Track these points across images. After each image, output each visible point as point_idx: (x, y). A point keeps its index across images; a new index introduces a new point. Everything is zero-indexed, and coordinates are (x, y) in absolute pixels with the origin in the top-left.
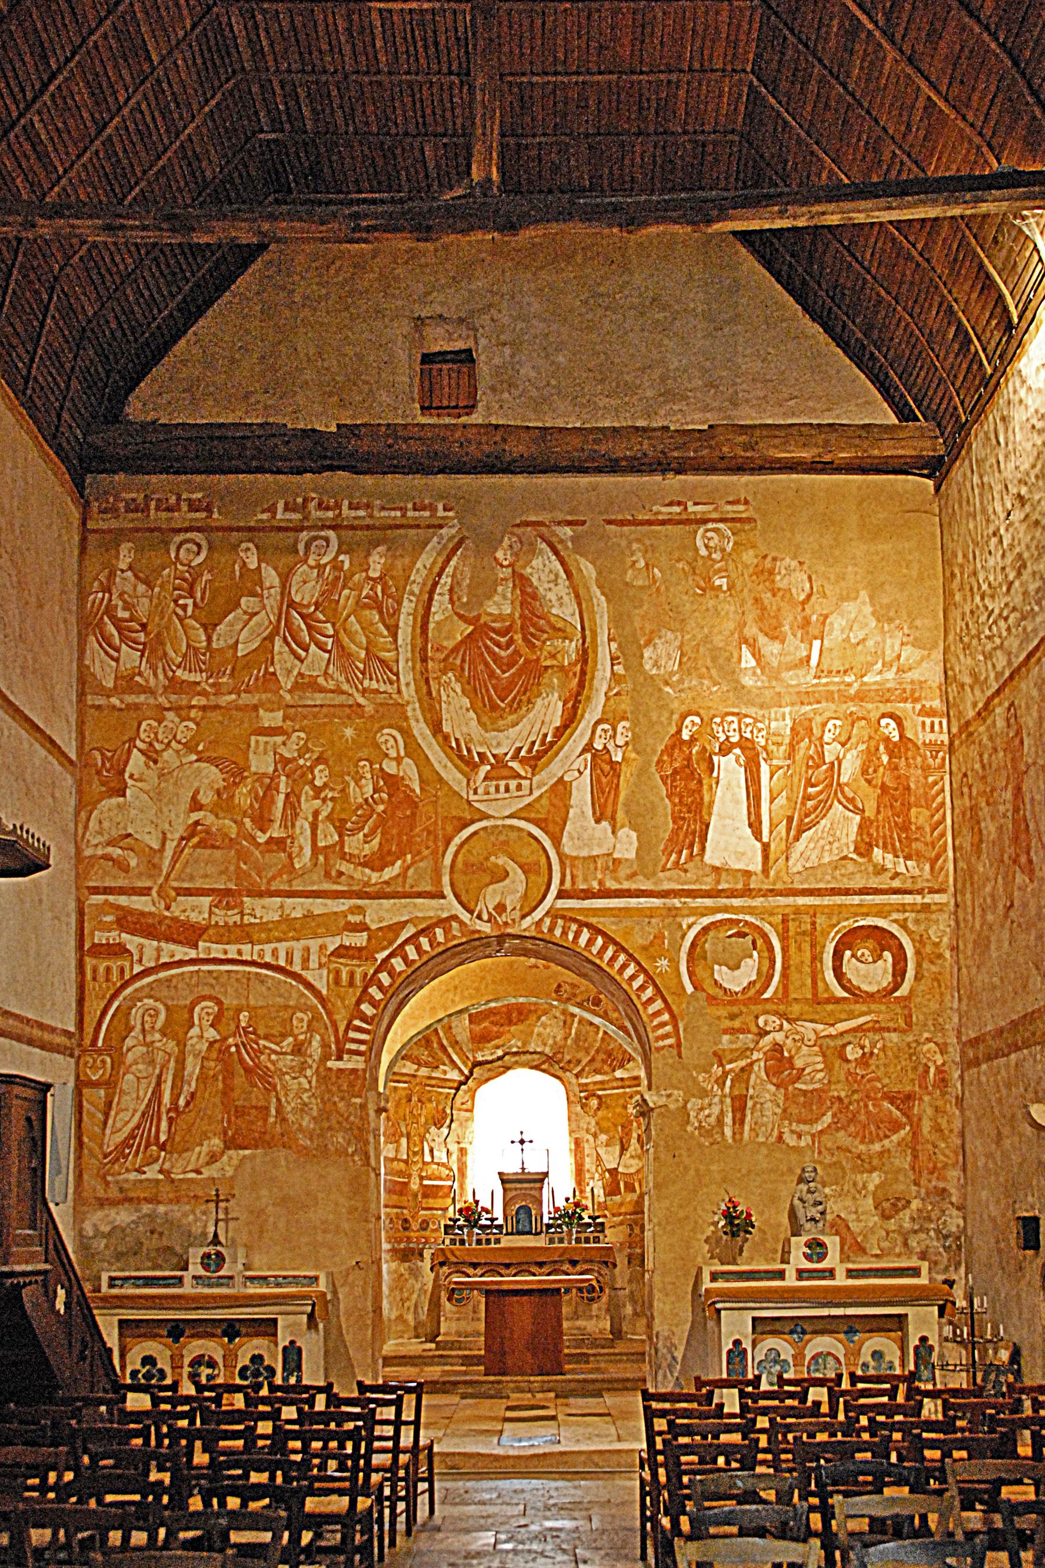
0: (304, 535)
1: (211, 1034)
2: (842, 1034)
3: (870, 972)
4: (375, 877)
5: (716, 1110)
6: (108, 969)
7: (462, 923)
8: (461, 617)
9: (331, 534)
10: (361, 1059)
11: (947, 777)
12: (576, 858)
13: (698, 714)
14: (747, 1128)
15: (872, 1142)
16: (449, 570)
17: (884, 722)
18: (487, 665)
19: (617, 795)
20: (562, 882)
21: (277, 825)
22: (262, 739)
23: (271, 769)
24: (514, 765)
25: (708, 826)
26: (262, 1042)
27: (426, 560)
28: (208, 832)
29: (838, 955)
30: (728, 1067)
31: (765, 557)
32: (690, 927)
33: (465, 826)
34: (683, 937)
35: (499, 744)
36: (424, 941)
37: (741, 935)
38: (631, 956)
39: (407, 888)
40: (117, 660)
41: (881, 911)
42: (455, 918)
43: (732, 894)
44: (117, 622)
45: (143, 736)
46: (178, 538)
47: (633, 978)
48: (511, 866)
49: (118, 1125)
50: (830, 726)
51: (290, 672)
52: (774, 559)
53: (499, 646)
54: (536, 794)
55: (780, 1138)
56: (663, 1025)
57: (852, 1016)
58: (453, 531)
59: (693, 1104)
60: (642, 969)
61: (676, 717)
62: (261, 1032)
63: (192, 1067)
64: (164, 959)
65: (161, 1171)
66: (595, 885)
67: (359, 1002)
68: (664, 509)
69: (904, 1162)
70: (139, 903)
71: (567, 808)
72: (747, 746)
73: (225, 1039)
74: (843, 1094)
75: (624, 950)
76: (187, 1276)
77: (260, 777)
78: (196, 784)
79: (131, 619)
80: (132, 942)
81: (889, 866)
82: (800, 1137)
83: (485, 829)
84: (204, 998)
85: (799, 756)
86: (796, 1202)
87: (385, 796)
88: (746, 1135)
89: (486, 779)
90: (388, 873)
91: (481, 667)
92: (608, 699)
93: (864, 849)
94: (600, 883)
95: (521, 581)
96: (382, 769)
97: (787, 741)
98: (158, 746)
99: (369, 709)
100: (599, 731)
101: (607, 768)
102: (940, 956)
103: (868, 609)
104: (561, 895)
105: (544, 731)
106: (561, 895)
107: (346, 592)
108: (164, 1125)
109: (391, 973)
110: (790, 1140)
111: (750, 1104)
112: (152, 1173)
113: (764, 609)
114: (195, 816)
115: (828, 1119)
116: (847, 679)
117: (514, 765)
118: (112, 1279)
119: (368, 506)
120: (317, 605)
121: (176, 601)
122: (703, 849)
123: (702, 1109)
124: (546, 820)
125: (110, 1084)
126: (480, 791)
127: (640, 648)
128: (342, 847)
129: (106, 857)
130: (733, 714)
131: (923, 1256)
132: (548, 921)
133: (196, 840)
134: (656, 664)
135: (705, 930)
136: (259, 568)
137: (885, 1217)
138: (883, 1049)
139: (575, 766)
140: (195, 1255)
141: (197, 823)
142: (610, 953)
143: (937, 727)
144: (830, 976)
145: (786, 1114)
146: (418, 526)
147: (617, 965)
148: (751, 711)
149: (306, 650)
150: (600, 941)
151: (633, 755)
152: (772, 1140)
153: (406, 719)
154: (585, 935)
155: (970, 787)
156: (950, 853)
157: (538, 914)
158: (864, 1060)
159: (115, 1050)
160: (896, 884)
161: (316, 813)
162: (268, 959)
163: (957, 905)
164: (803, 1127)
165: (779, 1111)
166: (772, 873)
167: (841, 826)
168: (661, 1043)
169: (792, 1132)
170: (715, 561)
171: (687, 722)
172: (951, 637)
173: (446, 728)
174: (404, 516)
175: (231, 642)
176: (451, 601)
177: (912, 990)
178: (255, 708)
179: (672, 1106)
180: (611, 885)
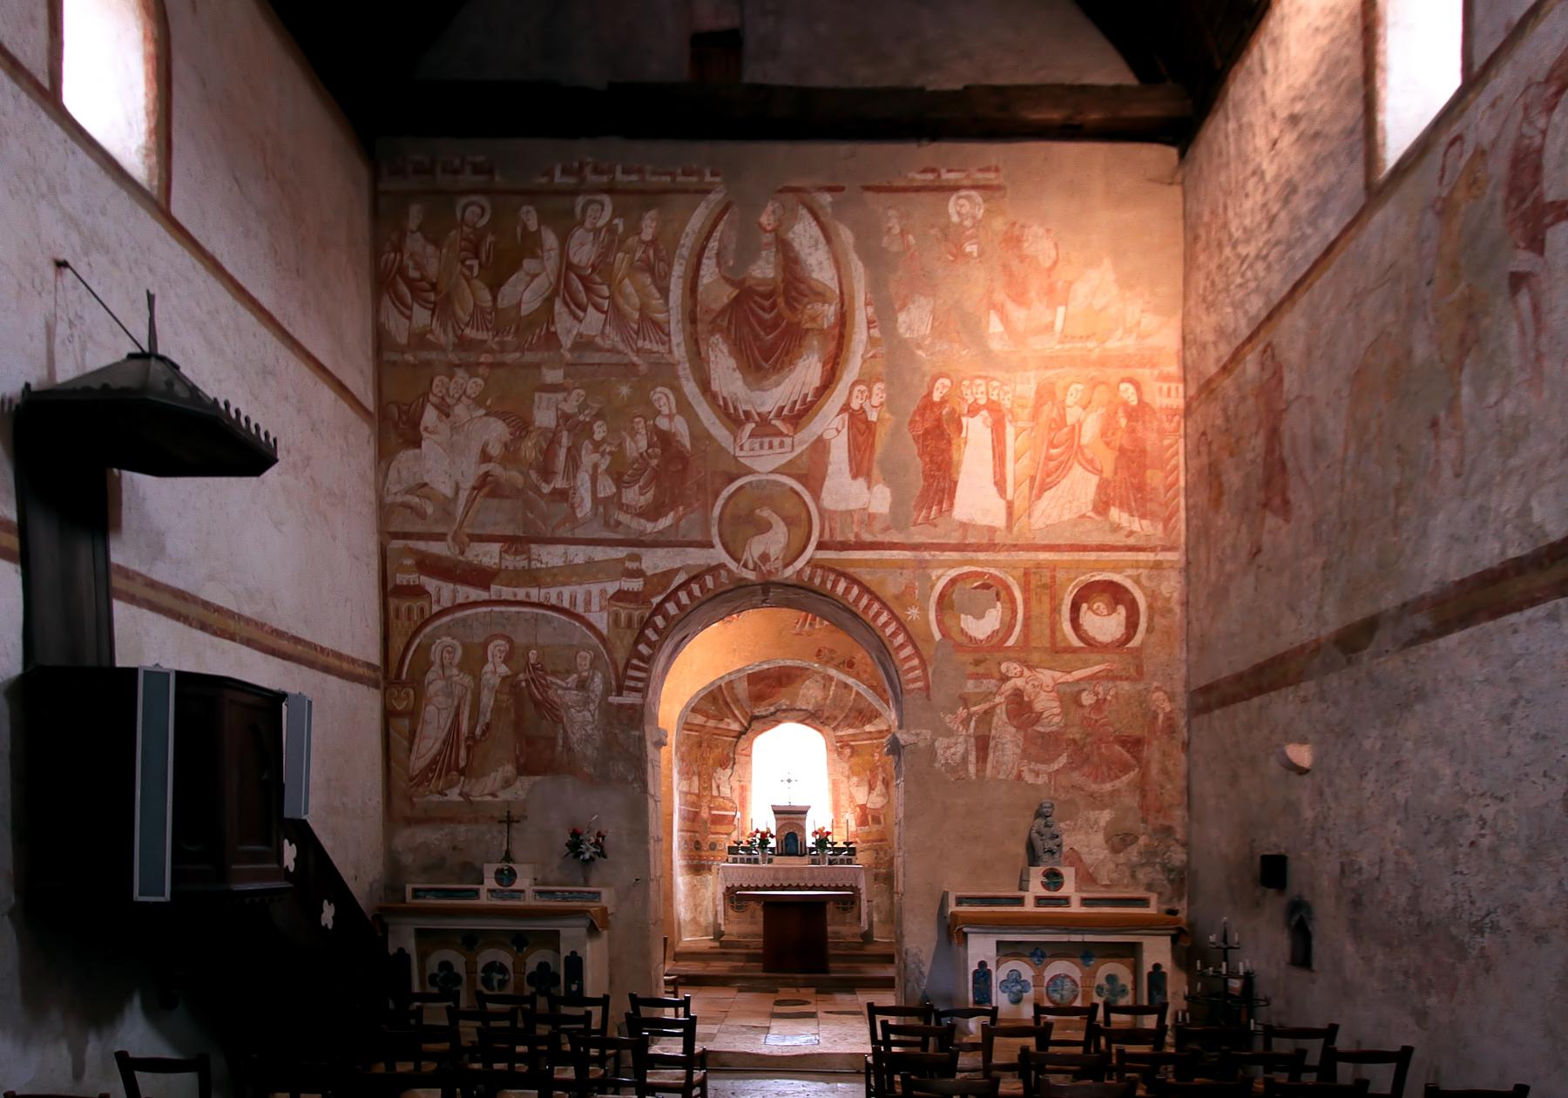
0: (581, 200)
1: (503, 669)
2: (1078, 681)
3: (1104, 624)
4: (649, 527)
5: (960, 749)
6: (410, 610)
7: (729, 571)
8: (727, 280)
9: (606, 199)
10: (638, 695)
11: (1182, 441)
12: (835, 512)
13: (948, 376)
14: (989, 766)
15: (1103, 781)
16: (717, 234)
17: (1123, 386)
18: (752, 328)
19: (872, 453)
20: (821, 535)
21: (559, 478)
22: (545, 396)
23: (553, 424)
24: (777, 423)
25: (956, 483)
26: (549, 678)
27: (697, 220)
28: (497, 483)
29: (1075, 608)
30: (973, 709)
31: (1014, 224)
32: (938, 578)
33: (732, 480)
34: (932, 587)
35: (763, 404)
36: (695, 588)
37: (986, 586)
38: (884, 605)
39: (680, 538)
40: (409, 318)
41: (1117, 567)
42: (723, 566)
43: (978, 548)
44: (410, 282)
45: (435, 390)
46: (463, 201)
47: (886, 625)
48: (776, 520)
49: (423, 751)
50: (1072, 388)
51: (569, 331)
52: (1023, 227)
53: (763, 309)
54: (798, 450)
55: (1019, 777)
56: (913, 669)
57: (1086, 665)
58: (720, 196)
59: (941, 743)
60: (894, 616)
61: (927, 379)
62: (549, 669)
63: (487, 700)
64: (460, 600)
65: (461, 794)
66: (852, 538)
67: (636, 643)
68: (919, 177)
69: (1131, 801)
70: (436, 548)
71: (826, 465)
72: (993, 408)
73: (517, 674)
74: (1078, 737)
75: (877, 598)
76: (483, 890)
77: (544, 431)
78: (485, 437)
79: (423, 279)
80: (431, 584)
81: (1125, 524)
82: (1038, 775)
83: (750, 483)
84: (496, 637)
85: (1043, 418)
86: (1035, 835)
87: (658, 450)
88: (988, 772)
89: (751, 436)
90: (665, 522)
91: (746, 330)
92: (864, 361)
93: (1102, 507)
94: (857, 535)
95: (785, 249)
96: (655, 425)
97: (1031, 403)
98: (448, 400)
99: (643, 368)
100: (856, 393)
101: (862, 427)
102: (1170, 610)
103: (1110, 276)
104: (821, 546)
105: (805, 391)
106: (821, 546)
107: (620, 255)
108: (463, 753)
109: (666, 617)
110: (1029, 778)
111: (992, 744)
112: (454, 795)
113: (1011, 275)
114: (485, 468)
115: (1063, 760)
116: (1091, 345)
117: (777, 423)
118: (415, 890)
119: (640, 171)
120: (594, 267)
121: (463, 262)
122: (952, 505)
123: (949, 747)
124: (806, 475)
125: (414, 714)
126: (746, 447)
127: (895, 313)
128: (620, 498)
129: (405, 505)
130: (980, 377)
131: (1149, 887)
132: (808, 571)
133: (486, 490)
134: (909, 328)
135: (953, 581)
136: (539, 231)
137: (1115, 850)
138: (1116, 696)
139: (834, 425)
140: (489, 871)
141: (487, 474)
142: (864, 601)
143: (1173, 392)
144: (1067, 627)
145: (1025, 755)
146: (686, 191)
147: (872, 613)
148: (999, 374)
149: (584, 310)
150: (855, 590)
151: (887, 415)
152: (1012, 777)
153: (677, 377)
154: (842, 586)
155: (1210, 444)
156: (1182, 514)
157: (800, 563)
158: (1099, 705)
159: (417, 683)
160: (1131, 541)
161: (596, 466)
162: (554, 601)
163: (1188, 563)
164: (1043, 767)
165: (1018, 751)
166: (1015, 529)
167: (1080, 487)
168: (912, 686)
169: (1031, 771)
170: (967, 229)
171: (938, 384)
172: (1192, 302)
173: (715, 387)
174: (673, 180)
175: (514, 302)
176: (719, 264)
177: (1143, 643)
178: (538, 366)
179: (921, 744)
180: (867, 537)
